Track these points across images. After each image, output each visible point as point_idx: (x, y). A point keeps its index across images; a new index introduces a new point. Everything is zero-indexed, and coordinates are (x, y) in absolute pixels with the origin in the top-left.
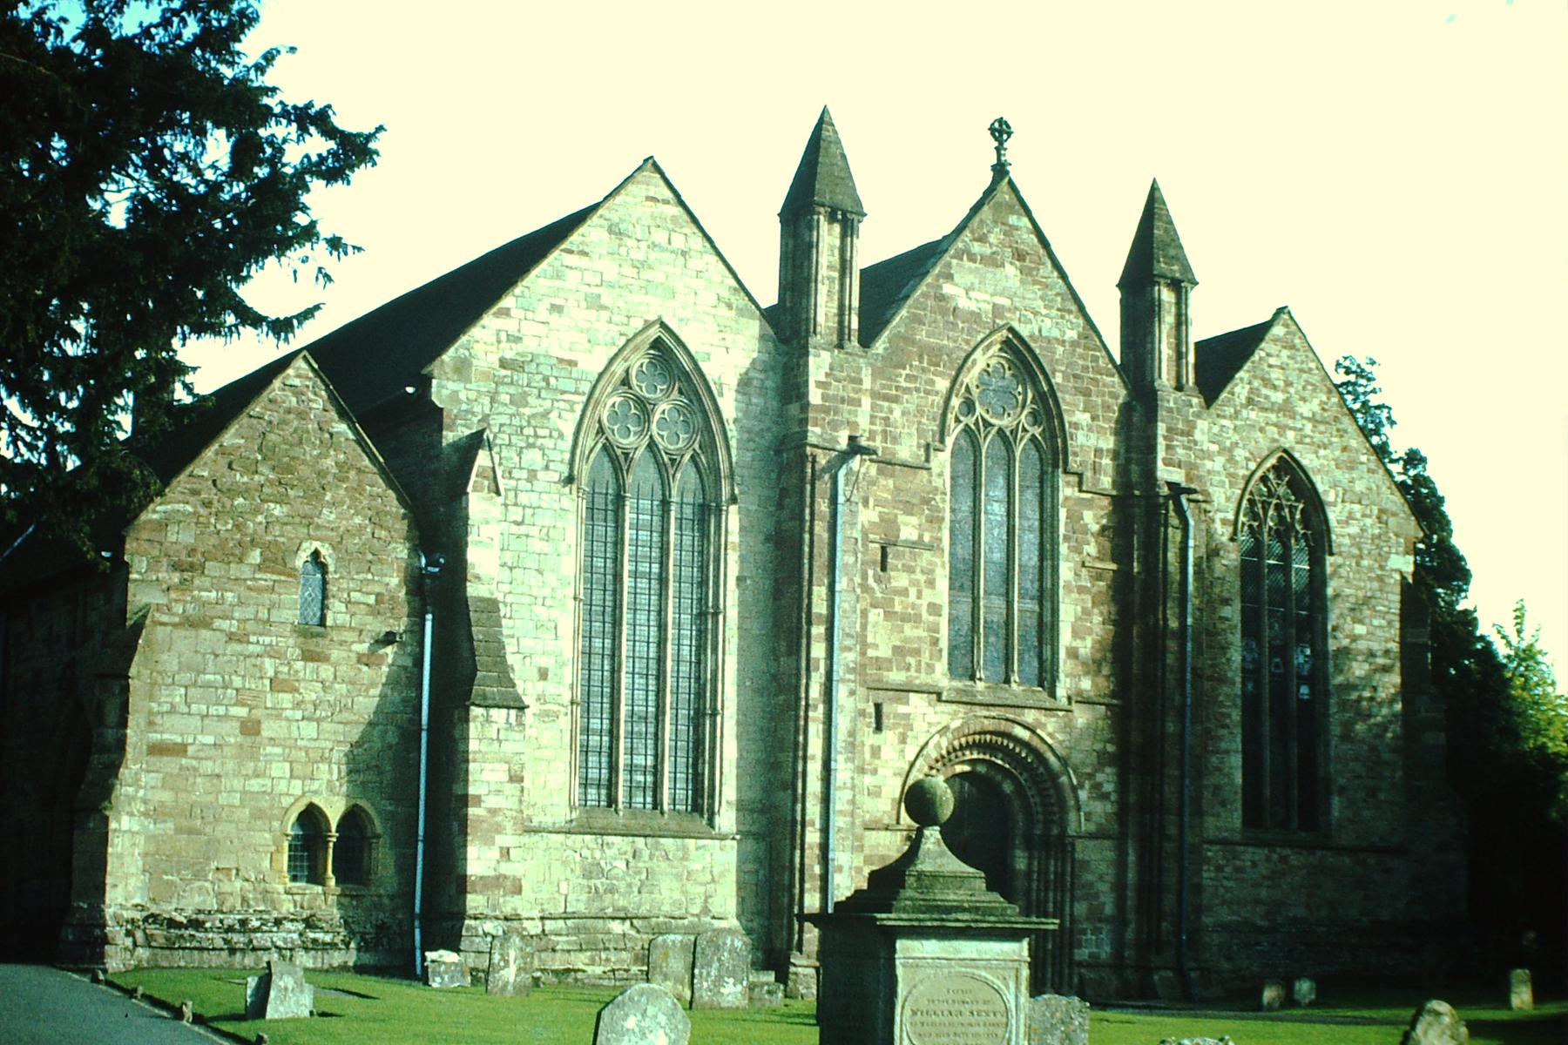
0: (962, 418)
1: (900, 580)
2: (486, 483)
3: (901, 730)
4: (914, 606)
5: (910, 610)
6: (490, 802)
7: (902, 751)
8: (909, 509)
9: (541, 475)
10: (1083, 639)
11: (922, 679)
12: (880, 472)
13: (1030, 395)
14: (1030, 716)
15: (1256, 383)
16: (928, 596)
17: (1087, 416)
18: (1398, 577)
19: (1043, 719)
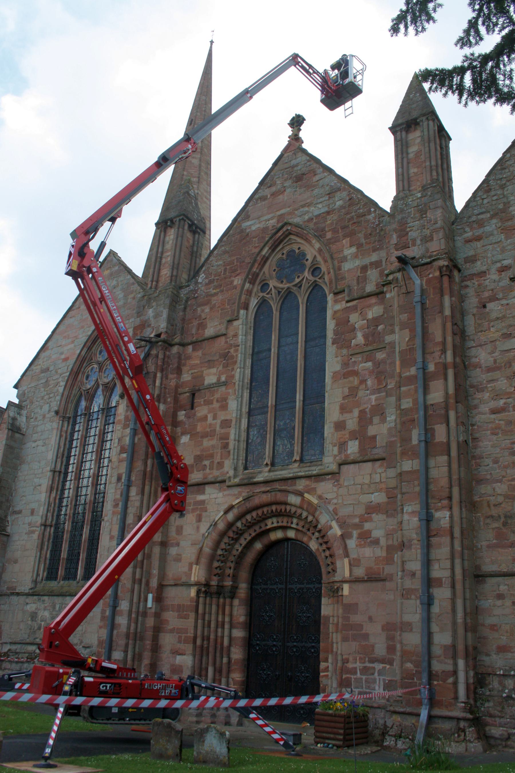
1: (201, 411)
3: (198, 512)
4: (210, 425)
7: (198, 528)
11: (215, 474)
16: (222, 416)
17: (353, 250)
19: (313, 485)
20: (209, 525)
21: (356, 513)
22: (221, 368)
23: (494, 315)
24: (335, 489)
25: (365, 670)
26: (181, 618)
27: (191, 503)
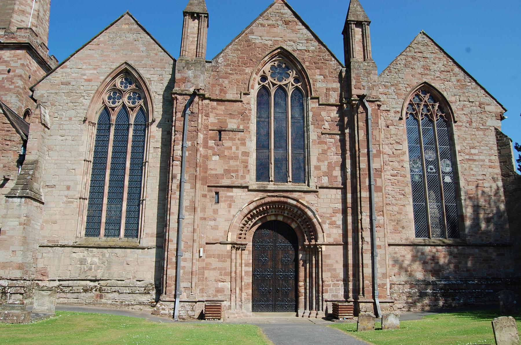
0: (261, 83)
1: (227, 143)
2: (38, 120)
3: (229, 202)
4: (234, 153)
5: (232, 155)
6: (10, 233)
7: (229, 211)
8: (231, 116)
9: (73, 119)
10: (323, 161)
12: (217, 104)
13: (295, 72)
14: (295, 195)
15: (410, 59)
16: (242, 149)
18: (493, 129)
20: (237, 210)
21: (328, 212)
22: (239, 120)
23: (393, 132)
24: (316, 199)
25: (335, 285)
26: (222, 261)
27: (223, 196)
